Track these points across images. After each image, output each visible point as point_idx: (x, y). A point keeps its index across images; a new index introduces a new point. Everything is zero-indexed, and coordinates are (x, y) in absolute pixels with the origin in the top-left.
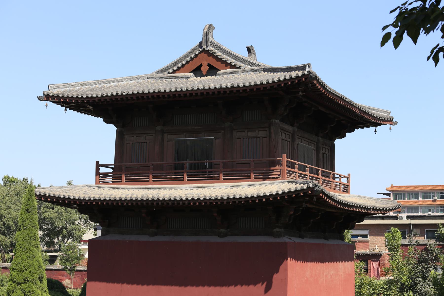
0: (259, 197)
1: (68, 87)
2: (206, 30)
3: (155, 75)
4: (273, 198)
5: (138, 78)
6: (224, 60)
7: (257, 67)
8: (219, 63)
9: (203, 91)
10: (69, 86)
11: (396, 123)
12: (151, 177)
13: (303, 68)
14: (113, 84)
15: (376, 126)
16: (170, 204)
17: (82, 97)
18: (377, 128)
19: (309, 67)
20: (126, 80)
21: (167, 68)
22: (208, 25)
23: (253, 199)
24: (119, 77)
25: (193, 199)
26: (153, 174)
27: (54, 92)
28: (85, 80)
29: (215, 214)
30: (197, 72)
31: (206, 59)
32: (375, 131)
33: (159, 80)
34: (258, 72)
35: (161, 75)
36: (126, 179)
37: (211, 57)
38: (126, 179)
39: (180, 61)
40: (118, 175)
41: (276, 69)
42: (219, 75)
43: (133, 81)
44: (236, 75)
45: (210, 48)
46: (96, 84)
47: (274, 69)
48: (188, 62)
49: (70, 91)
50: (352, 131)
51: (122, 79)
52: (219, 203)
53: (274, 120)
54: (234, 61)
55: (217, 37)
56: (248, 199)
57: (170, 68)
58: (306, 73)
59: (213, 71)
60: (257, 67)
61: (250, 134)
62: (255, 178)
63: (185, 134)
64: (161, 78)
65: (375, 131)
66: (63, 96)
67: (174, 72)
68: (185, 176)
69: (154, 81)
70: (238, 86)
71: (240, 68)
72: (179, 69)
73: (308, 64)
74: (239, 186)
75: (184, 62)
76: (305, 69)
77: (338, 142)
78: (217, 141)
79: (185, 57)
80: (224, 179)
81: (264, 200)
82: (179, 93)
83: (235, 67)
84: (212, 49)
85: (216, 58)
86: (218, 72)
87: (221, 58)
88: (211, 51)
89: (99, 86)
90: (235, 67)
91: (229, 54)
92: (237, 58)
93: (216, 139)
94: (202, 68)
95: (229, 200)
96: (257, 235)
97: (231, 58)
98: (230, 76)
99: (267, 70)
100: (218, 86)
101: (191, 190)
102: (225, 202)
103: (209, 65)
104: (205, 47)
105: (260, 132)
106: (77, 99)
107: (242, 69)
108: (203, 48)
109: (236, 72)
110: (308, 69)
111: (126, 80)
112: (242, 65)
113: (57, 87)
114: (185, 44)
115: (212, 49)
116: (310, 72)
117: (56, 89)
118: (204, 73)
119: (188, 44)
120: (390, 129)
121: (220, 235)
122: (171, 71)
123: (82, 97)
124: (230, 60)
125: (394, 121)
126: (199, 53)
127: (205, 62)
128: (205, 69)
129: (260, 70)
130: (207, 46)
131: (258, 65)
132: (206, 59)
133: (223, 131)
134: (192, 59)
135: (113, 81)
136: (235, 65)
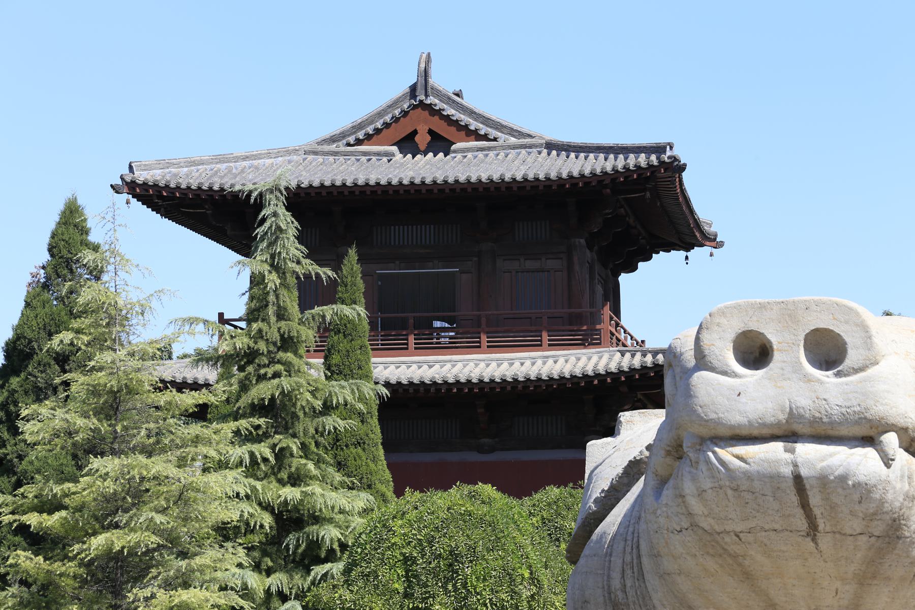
0: (585, 376)
1: (168, 167)
2: (423, 66)
3: (320, 148)
4: (612, 379)
5: (288, 152)
6: (463, 124)
7: (528, 141)
8: (453, 129)
9: (466, 186)
10: (169, 164)
11: (720, 245)
12: (545, 336)
13: (659, 149)
14: (246, 163)
15: (688, 250)
16: (411, 391)
17: (211, 189)
18: (689, 254)
19: (671, 148)
20: (268, 155)
21: (343, 135)
22: (424, 56)
23: (575, 380)
24: (254, 149)
25: (458, 382)
26: (487, 333)
27: (141, 176)
28: (195, 155)
29: (481, 410)
30: (408, 144)
31: (424, 120)
32: (687, 258)
33: (331, 158)
34: (535, 150)
35: (333, 147)
36: (488, 342)
37: (437, 117)
38: (415, 344)
39: (370, 121)
40: (532, 332)
41: (580, 147)
42: (455, 152)
43: (280, 159)
44: (492, 154)
45: (431, 100)
46: (217, 163)
47: (574, 147)
48: (387, 125)
49: (175, 175)
50: (648, 258)
51: (260, 154)
52: (509, 388)
53: (577, 240)
54: (481, 126)
55: (436, 80)
56: (564, 381)
57: (349, 135)
58: (665, 158)
59: (440, 144)
60: (528, 141)
61: (530, 264)
62: (549, 345)
63: (397, 262)
64: (335, 154)
65: (687, 258)
66: (167, 186)
67: (359, 142)
68: (412, 339)
69: (320, 159)
70: (537, 179)
71: (495, 139)
72: (369, 137)
73: (669, 144)
74: (492, 360)
75: (379, 125)
76: (665, 152)
77: (624, 279)
78: (464, 276)
79: (380, 114)
80: (488, 347)
81: (609, 380)
82: (417, 188)
83: (485, 138)
84: (437, 101)
85: (447, 119)
86: (453, 147)
87: (457, 121)
88: (435, 105)
89: (223, 166)
90: (485, 138)
91: (471, 113)
92: (487, 121)
93: (462, 272)
94: (417, 138)
95: (529, 383)
96: (552, 448)
97: (475, 120)
98: (481, 155)
99: (551, 146)
100: (496, 177)
101: (430, 367)
102: (520, 386)
103: (431, 132)
104: (423, 97)
105: (548, 261)
106: (199, 192)
107: (501, 142)
108: (418, 99)
109: (489, 149)
110: (669, 153)
111: (268, 155)
112: (500, 134)
113: (148, 168)
114: (381, 89)
115: (437, 101)
116: (675, 159)
117: (145, 170)
118: (422, 147)
119: (386, 89)
120: (711, 255)
121: (480, 450)
122: (351, 139)
123: (211, 189)
124: (474, 125)
125: (718, 240)
126: (412, 109)
127: (423, 127)
128: (422, 139)
129: (541, 145)
130: (427, 96)
131: (530, 136)
132: (424, 120)
133: (476, 259)
134: (396, 120)
135: (246, 158)
136: (486, 135)
